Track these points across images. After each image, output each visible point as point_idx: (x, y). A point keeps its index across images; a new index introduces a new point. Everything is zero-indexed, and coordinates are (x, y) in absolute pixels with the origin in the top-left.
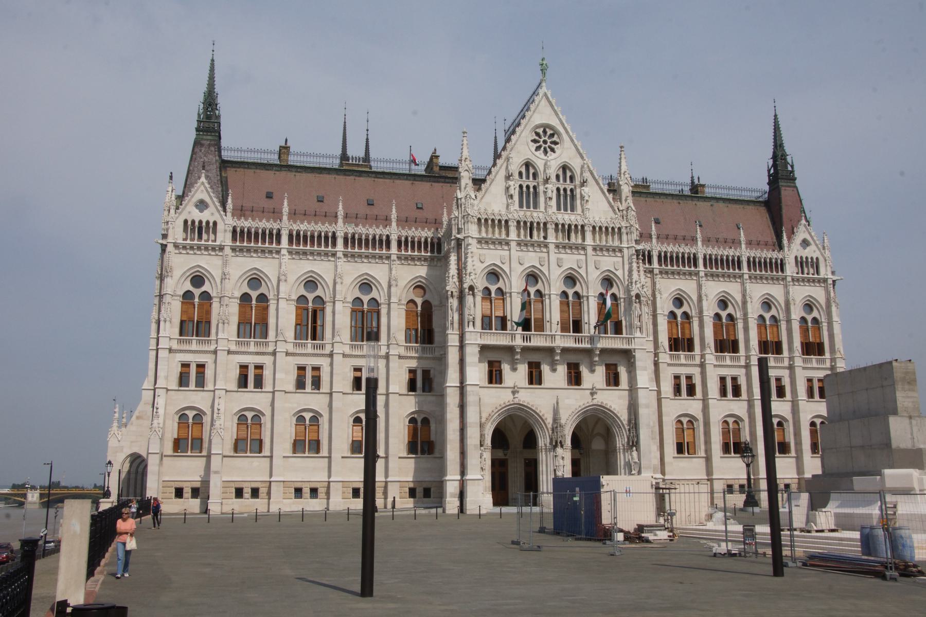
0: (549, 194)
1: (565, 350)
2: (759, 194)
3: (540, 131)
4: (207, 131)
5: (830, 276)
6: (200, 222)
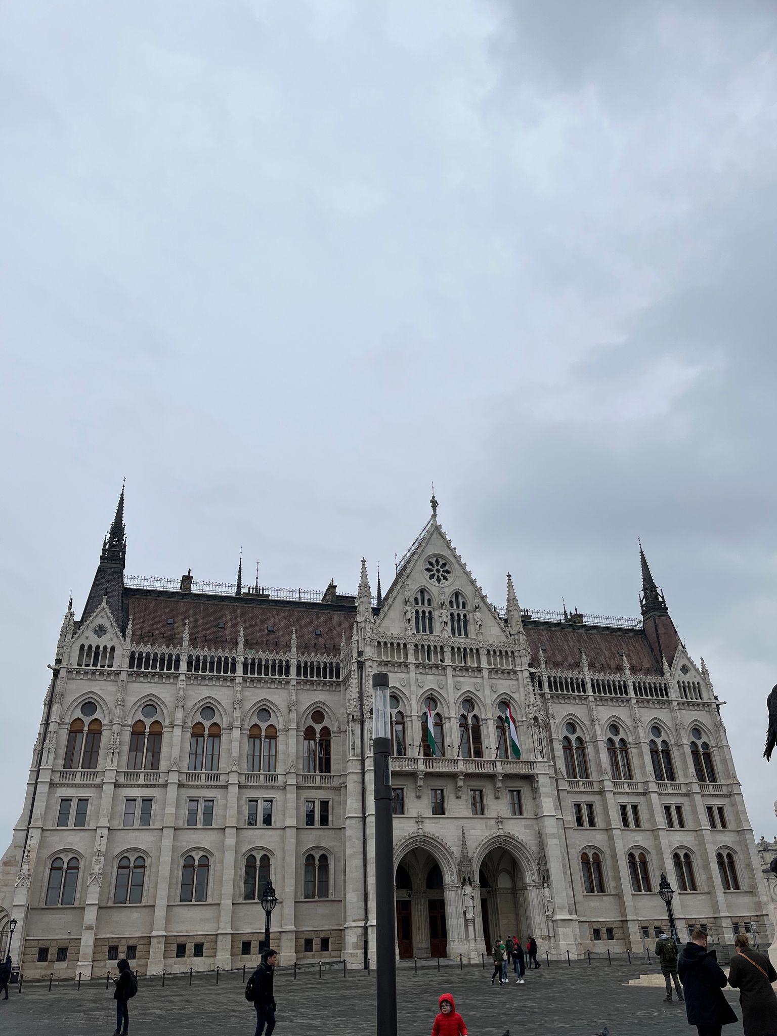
2: (633, 624)
4: (112, 560)
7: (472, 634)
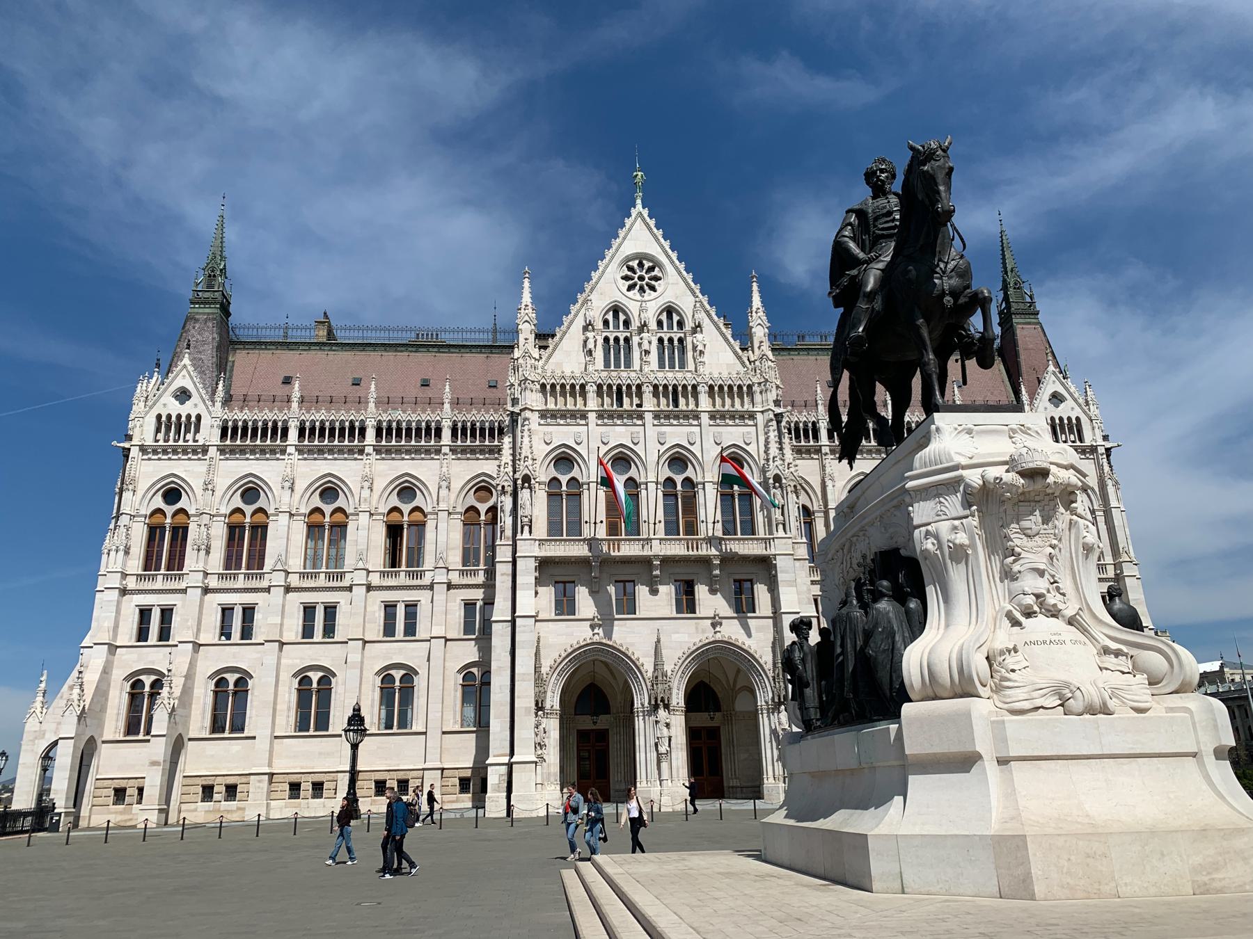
0: (646, 346)
1: (667, 561)
3: (635, 264)
5: (1100, 442)
6: (179, 416)
7: (691, 366)
